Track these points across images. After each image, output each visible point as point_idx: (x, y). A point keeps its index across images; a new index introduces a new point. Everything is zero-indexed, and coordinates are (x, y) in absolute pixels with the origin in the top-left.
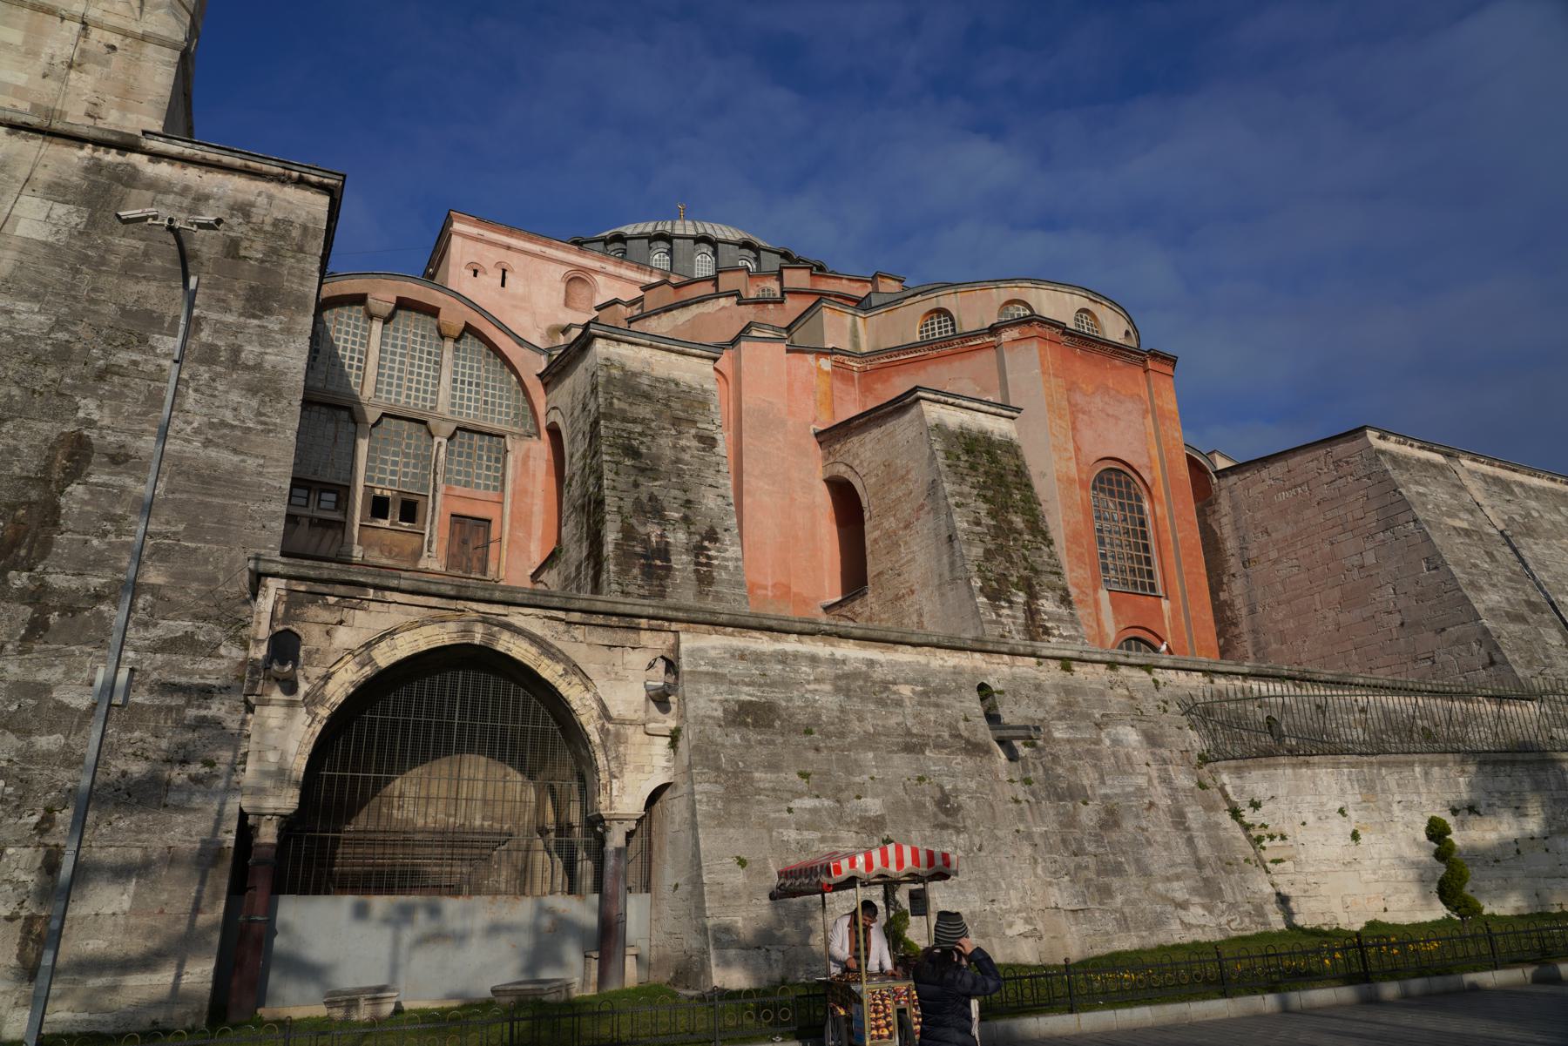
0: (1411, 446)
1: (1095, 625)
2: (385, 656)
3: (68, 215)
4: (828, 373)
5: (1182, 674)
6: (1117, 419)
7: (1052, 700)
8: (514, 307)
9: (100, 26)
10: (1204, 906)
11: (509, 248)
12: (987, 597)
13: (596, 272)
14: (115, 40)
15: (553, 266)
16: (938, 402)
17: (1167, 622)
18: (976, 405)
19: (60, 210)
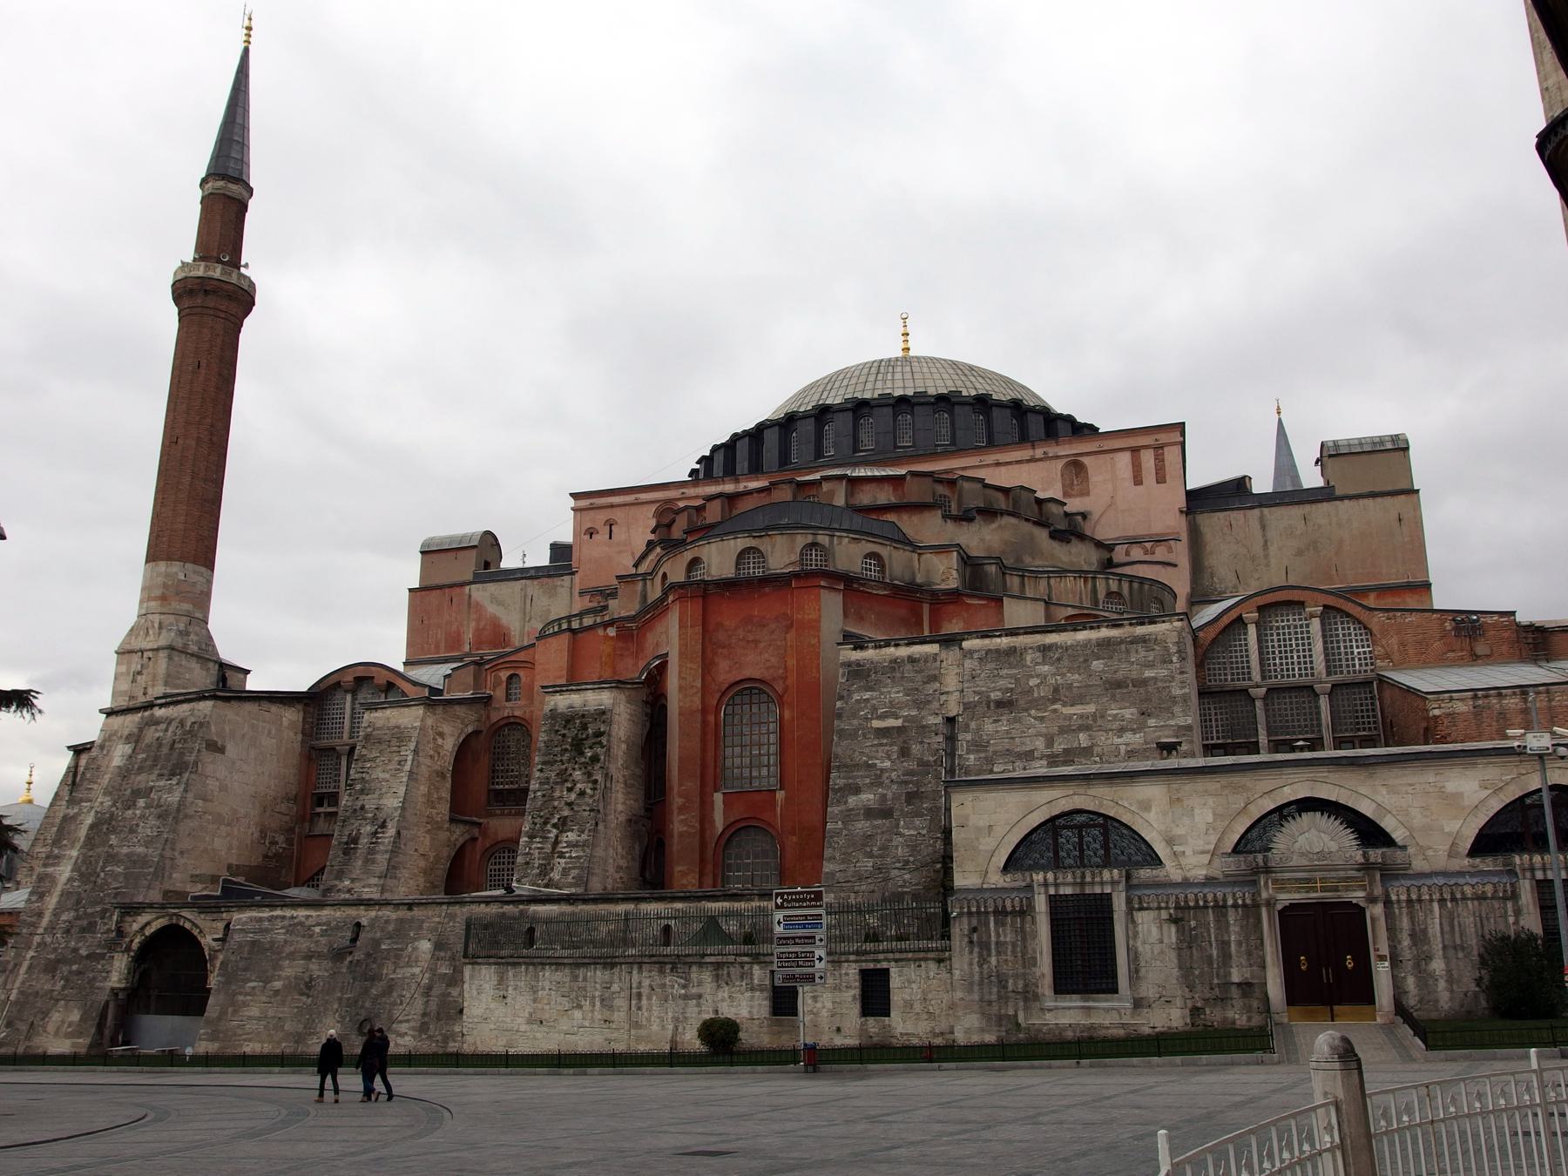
0: (897, 645)
1: (697, 825)
2: (148, 932)
3: (128, 749)
4: (612, 638)
5: (483, 906)
6: (756, 642)
7: (391, 928)
8: (620, 552)
9: (147, 650)
10: (413, 1036)
11: (612, 506)
12: (529, 837)
13: (679, 499)
14: (150, 654)
15: (645, 508)
16: (557, 692)
17: (779, 809)
18: (583, 687)
19: (127, 746)
